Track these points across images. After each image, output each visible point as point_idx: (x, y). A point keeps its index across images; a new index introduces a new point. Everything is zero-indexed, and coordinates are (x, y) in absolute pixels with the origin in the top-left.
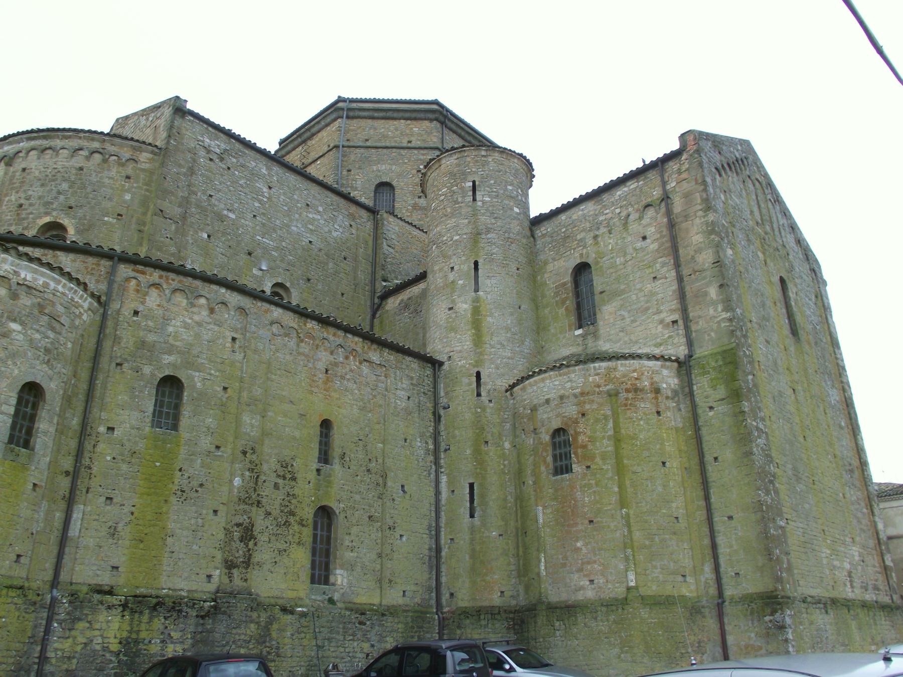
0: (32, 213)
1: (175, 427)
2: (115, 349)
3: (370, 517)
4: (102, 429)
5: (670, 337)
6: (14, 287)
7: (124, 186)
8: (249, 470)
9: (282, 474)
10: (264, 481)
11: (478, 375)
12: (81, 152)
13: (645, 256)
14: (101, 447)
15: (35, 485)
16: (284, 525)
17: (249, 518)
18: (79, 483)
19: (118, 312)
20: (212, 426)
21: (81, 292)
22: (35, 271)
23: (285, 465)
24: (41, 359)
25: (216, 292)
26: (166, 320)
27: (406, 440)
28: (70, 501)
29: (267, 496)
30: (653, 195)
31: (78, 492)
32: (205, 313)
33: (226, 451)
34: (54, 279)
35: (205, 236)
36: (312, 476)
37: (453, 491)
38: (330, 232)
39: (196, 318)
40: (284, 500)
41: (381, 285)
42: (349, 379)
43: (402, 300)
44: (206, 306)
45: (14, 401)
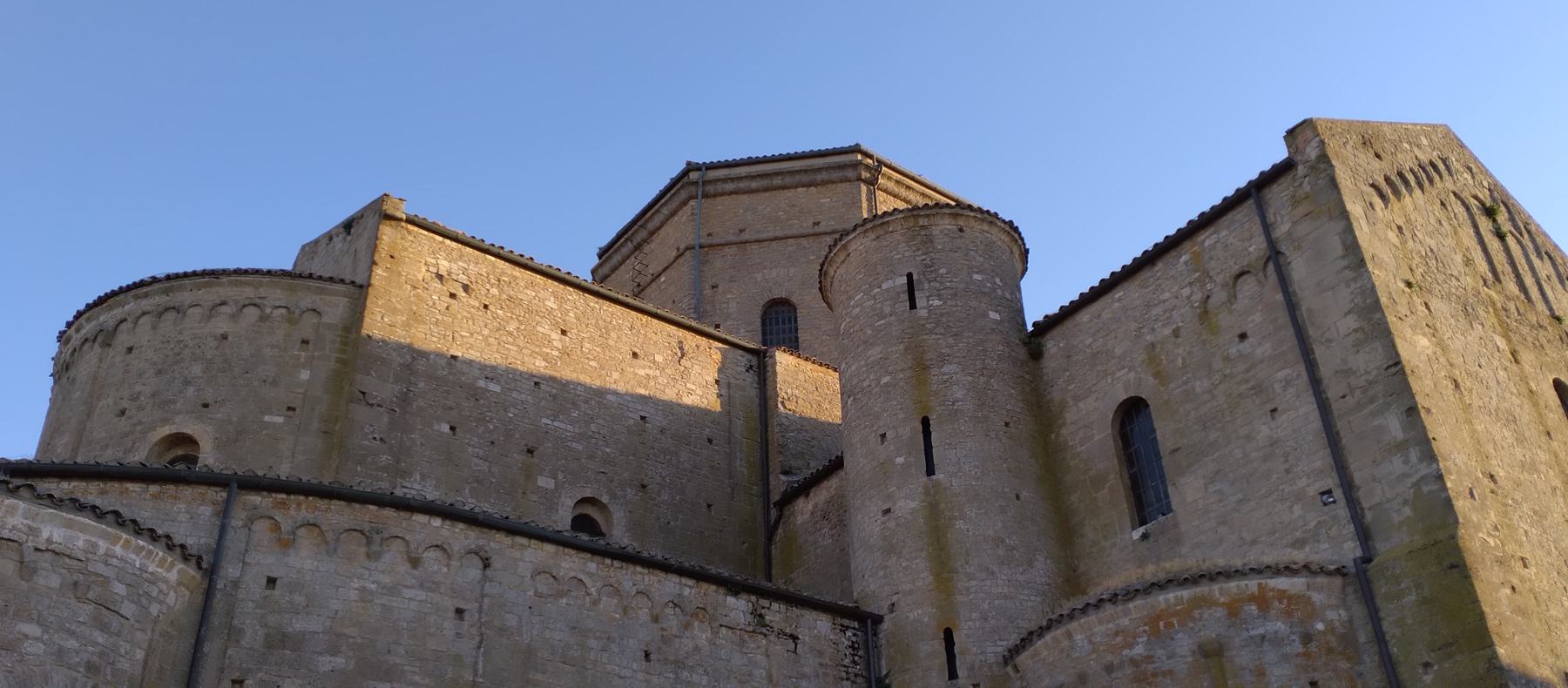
0: (140, 423)
2: (230, 652)
6: (30, 556)
13: (1248, 370)
21: (161, 554)
30: (1250, 253)
34: (105, 536)
39: (386, 579)
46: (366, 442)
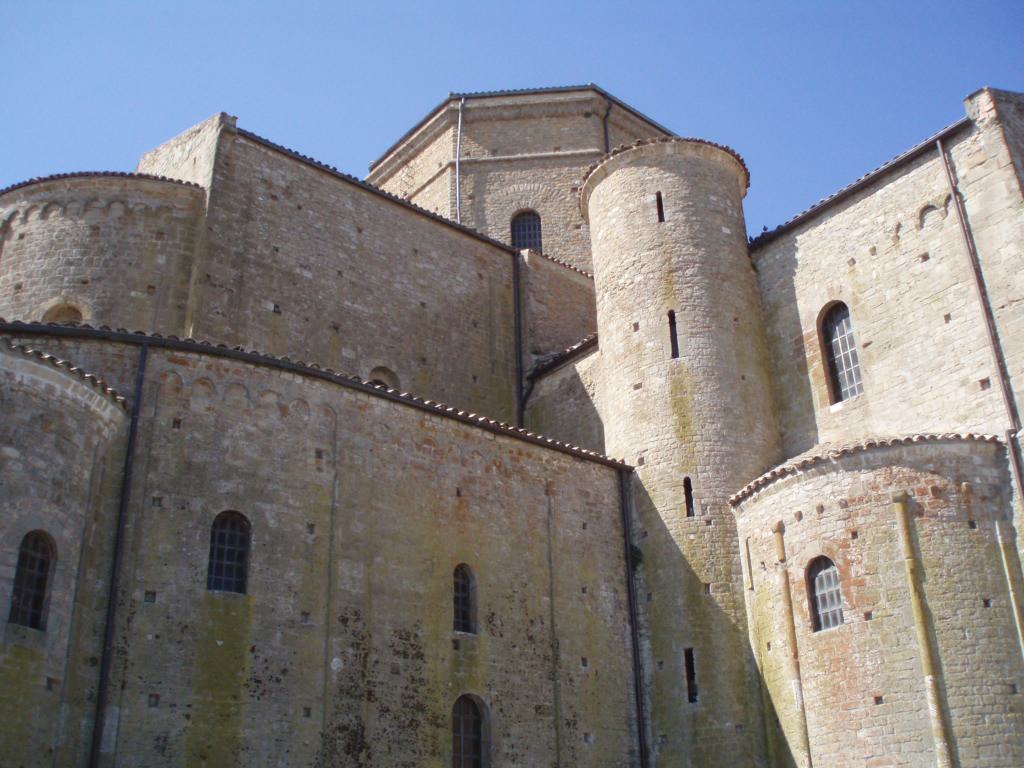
1: (241, 587)
3: (538, 708)
4: (138, 595)
5: (979, 405)
7: (156, 245)
8: (352, 645)
9: (401, 649)
10: (377, 662)
11: (687, 483)
12: (96, 204)
14: (139, 622)
15: (50, 681)
16: (410, 725)
17: (356, 717)
18: (110, 676)
19: (152, 422)
20: (294, 582)
21: (99, 397)
22: (35, 371)
23: (405, 636)
24: (49, 495)
25: (289, 383)
26: (221, 428)
27: (584, 591)
28: (100, 702)
29: (382, 683)
31: (110, 688)
32: (274, 416)
33: (318, 620)
35: (271, 307)
36: (447, 651)
37: (661, 663)
38: (450, 286)
39: (263, 424)
40: (406, 688)
41: (531, 361)
42: (492, 502)
43: (564, 380)
44: (276, 406)
45: (14, 560)
46: (211, 316)
